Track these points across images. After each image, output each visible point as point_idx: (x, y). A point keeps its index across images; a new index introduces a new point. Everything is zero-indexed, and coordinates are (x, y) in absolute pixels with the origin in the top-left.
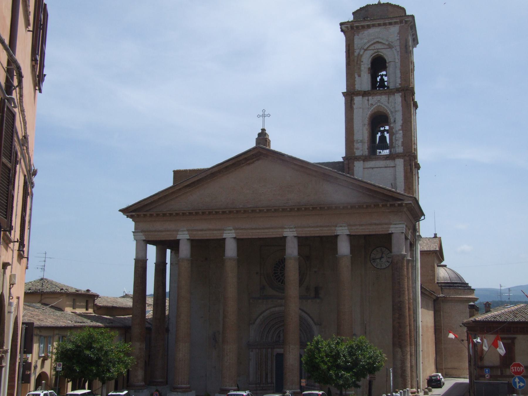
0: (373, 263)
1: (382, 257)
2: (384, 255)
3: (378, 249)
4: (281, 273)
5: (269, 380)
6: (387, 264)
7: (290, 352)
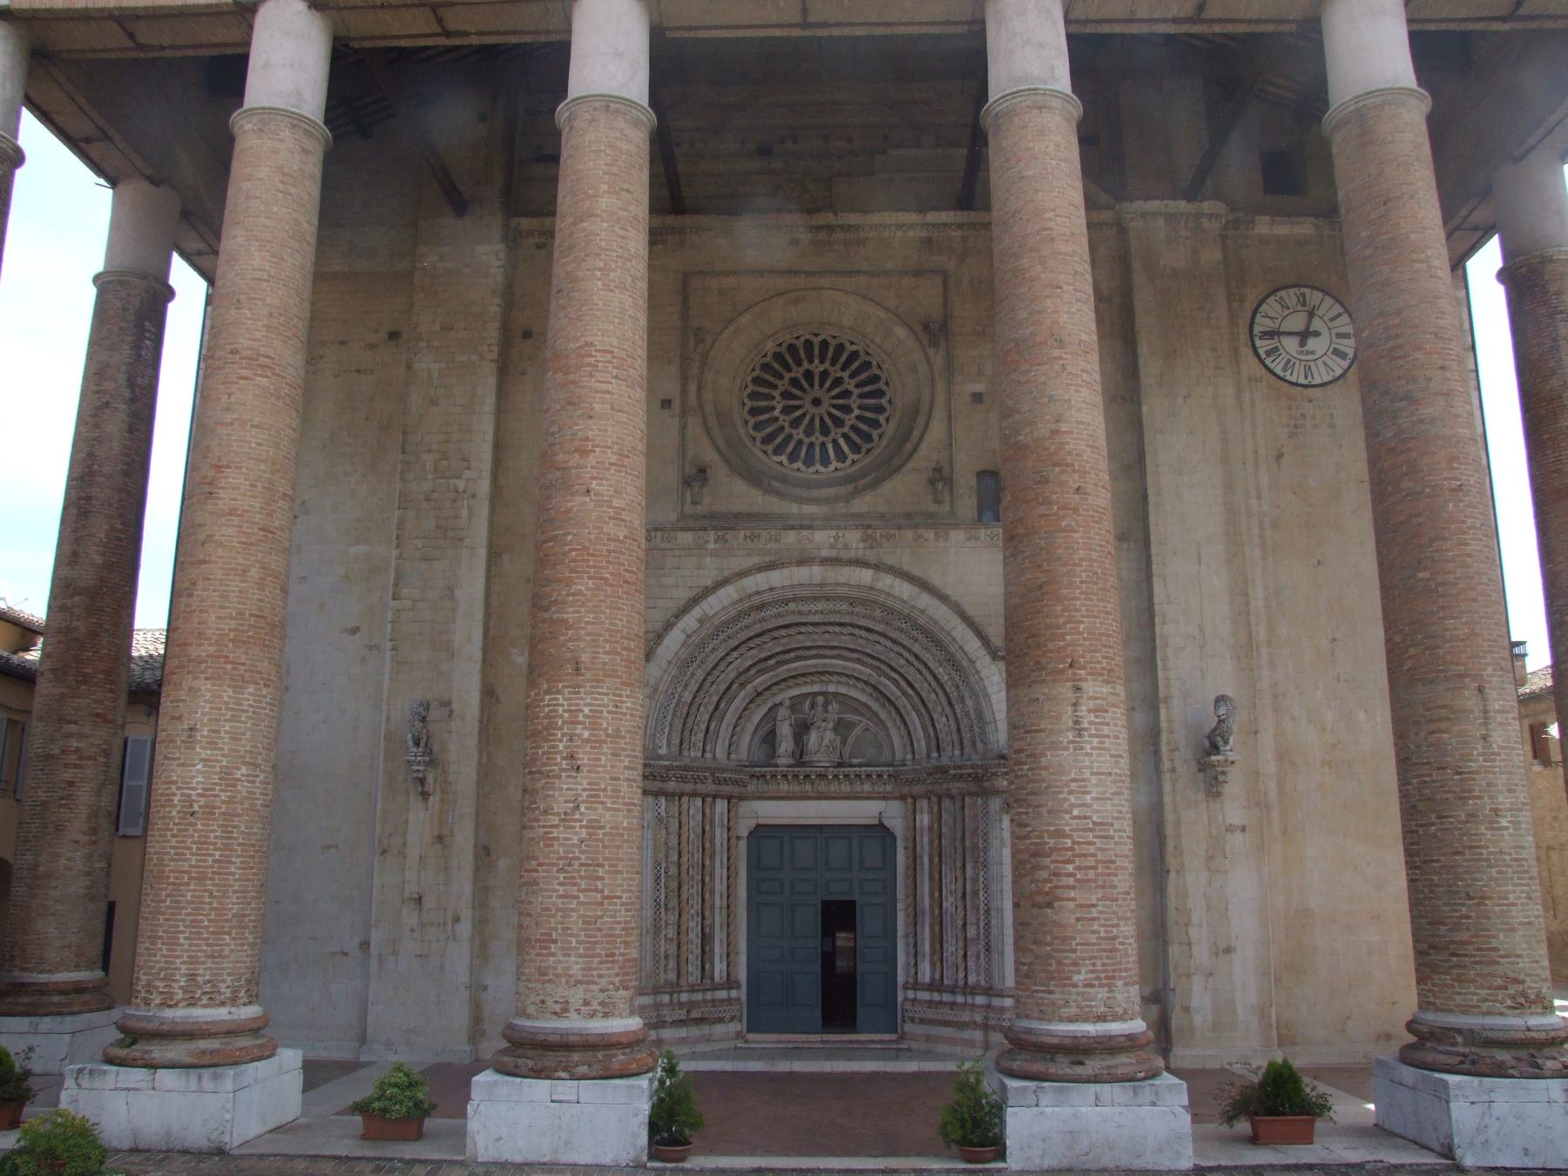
0: (1268, 361)
1: (1304, 335)
2: (1316, 324)
3: (1290, 296)
4: (787, 410)
5: (719, 968)
6: (1339, 366)
7: (1079, 732)
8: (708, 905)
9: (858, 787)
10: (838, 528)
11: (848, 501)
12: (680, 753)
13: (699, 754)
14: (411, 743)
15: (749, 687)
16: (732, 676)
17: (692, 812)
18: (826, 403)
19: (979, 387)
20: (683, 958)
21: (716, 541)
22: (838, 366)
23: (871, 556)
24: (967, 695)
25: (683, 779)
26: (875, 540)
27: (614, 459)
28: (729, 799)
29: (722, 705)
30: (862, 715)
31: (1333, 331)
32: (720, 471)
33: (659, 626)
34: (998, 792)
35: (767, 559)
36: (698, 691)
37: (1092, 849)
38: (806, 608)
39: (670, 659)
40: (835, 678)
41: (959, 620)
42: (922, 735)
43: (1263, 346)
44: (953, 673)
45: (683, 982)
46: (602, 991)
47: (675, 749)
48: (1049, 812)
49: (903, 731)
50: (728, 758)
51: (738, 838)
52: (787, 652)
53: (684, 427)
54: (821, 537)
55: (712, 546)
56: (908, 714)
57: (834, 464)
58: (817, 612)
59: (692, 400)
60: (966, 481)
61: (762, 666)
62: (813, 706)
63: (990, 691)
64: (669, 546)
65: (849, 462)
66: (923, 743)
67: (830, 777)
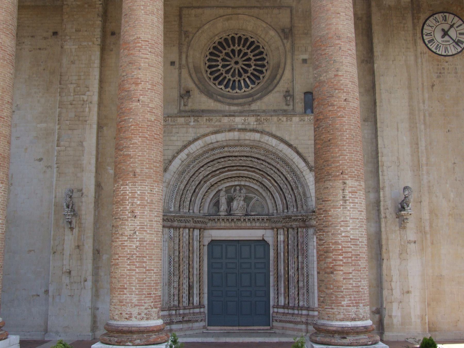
0: (429, 45)
3: (439, 17)
4: (224, 66)
5: (196, 300)
8: (191, 274)
9: (254, 224)
10: (246, 116)
11: (250, 105)
12: (179, 210)
13: (187, 211)
14: (65, 207)
15: (208, 183)
16: (201, 178)
17: (184, 235)
18: (241, 63)
19: (305, 57)
20: (181, 295)
21: (194, 122)
22: (246, 48)
23: (259, 128)
24: (299, 186)
25: (181, 221)
26: (261, 121)
27: (150, 87)
28: (200, 229)
29: (197, 190)
30: (256, 194)
31: (458, 32)
32: (196, 93)
33: (170, 157)
34: (312, 226)
35: (215, 129)
36: (187, 184)
37: (350, 250)
38: (232, 149)
39: (175, 171)
40: (244, 179)
41: (296, 155)
42: (280, 203)
43: (427, 39)
44: (294, 177)
45: (181, 305)
46: (146, 309)
47: (177, 208)
48: (332, 234)
49: (273, 201)
50: (200, 212)
51: (204, 245)
52: (224, 168)
53: (180, 73)
54: (238, 120)
55: (192, 124)
56: (275, 194)
57: (244, 89)
58: (236, 151)
59: (184, 62)
60: (299, 97)
61: (213, 174)
62: (235, 190)
63: (309, 184)
64: (174, 124)
65: (250, 88)
66: (281, 206)
67: (242, 220)
